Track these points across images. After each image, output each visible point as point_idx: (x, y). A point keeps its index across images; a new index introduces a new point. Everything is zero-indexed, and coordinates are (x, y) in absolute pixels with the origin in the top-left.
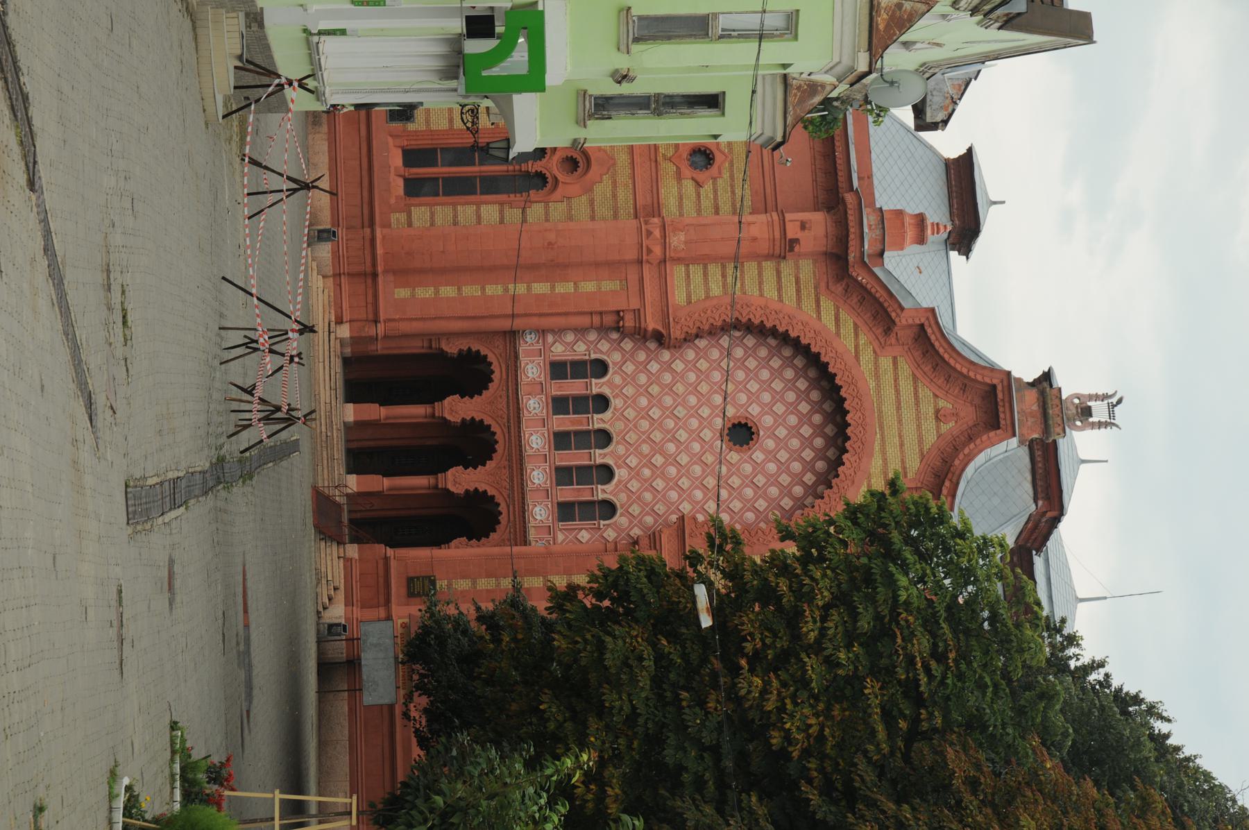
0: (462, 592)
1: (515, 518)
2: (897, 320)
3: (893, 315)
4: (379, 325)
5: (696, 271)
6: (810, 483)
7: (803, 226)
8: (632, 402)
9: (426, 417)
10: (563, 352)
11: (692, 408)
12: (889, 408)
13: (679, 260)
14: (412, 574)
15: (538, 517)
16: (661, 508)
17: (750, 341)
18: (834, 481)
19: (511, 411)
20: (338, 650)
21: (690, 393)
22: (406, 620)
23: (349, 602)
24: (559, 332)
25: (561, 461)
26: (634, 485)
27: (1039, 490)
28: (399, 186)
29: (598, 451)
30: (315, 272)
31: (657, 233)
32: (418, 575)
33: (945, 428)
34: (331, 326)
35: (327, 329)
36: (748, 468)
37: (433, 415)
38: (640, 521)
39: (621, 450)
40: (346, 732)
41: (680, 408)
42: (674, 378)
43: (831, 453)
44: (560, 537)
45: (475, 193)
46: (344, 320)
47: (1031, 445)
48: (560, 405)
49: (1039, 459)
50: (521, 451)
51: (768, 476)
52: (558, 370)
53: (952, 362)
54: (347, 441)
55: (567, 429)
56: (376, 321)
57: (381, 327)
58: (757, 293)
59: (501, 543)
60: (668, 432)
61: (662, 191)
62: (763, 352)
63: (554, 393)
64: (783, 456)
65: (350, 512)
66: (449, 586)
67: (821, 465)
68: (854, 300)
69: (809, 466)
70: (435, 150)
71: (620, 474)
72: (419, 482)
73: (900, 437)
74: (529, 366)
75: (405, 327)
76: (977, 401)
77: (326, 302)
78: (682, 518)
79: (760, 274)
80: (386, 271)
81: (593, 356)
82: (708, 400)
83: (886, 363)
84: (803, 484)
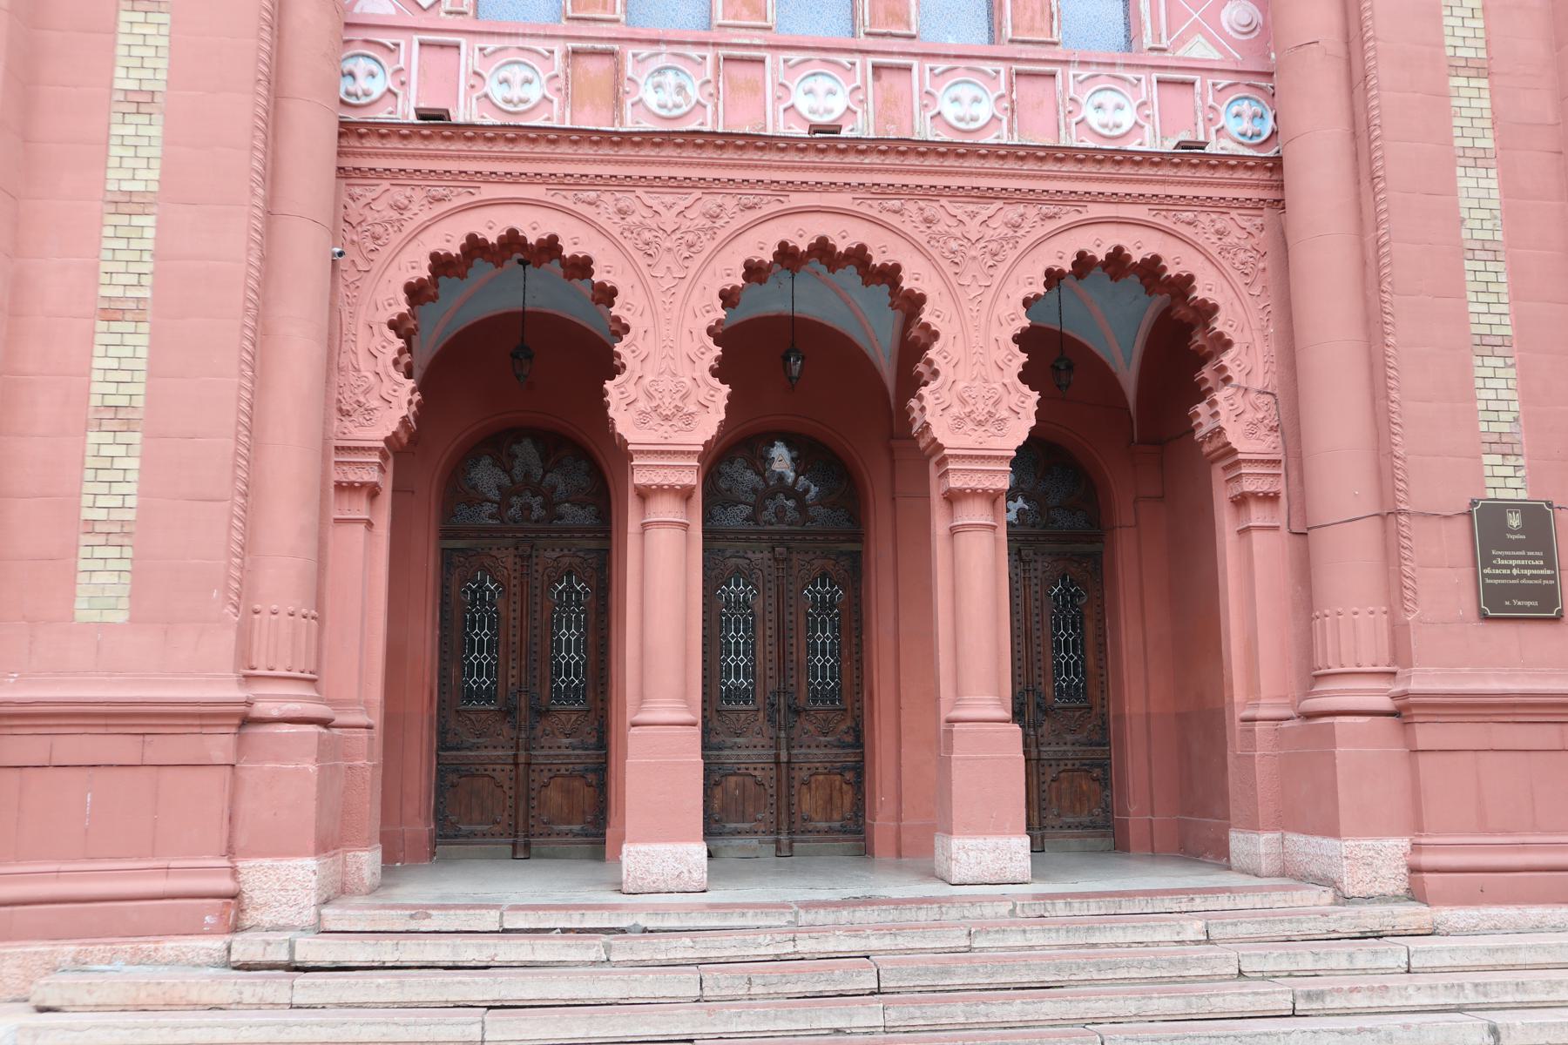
0: (1527, 397)
1: (1140, 199)
4: (262, 709)
15: (1127, 118)
19: (695, 173)
35: (277, 987)
44: (1199, 50)
46: (225, 884)
63: (619, 13)
66: (1503, 446)
74: (498, 93)
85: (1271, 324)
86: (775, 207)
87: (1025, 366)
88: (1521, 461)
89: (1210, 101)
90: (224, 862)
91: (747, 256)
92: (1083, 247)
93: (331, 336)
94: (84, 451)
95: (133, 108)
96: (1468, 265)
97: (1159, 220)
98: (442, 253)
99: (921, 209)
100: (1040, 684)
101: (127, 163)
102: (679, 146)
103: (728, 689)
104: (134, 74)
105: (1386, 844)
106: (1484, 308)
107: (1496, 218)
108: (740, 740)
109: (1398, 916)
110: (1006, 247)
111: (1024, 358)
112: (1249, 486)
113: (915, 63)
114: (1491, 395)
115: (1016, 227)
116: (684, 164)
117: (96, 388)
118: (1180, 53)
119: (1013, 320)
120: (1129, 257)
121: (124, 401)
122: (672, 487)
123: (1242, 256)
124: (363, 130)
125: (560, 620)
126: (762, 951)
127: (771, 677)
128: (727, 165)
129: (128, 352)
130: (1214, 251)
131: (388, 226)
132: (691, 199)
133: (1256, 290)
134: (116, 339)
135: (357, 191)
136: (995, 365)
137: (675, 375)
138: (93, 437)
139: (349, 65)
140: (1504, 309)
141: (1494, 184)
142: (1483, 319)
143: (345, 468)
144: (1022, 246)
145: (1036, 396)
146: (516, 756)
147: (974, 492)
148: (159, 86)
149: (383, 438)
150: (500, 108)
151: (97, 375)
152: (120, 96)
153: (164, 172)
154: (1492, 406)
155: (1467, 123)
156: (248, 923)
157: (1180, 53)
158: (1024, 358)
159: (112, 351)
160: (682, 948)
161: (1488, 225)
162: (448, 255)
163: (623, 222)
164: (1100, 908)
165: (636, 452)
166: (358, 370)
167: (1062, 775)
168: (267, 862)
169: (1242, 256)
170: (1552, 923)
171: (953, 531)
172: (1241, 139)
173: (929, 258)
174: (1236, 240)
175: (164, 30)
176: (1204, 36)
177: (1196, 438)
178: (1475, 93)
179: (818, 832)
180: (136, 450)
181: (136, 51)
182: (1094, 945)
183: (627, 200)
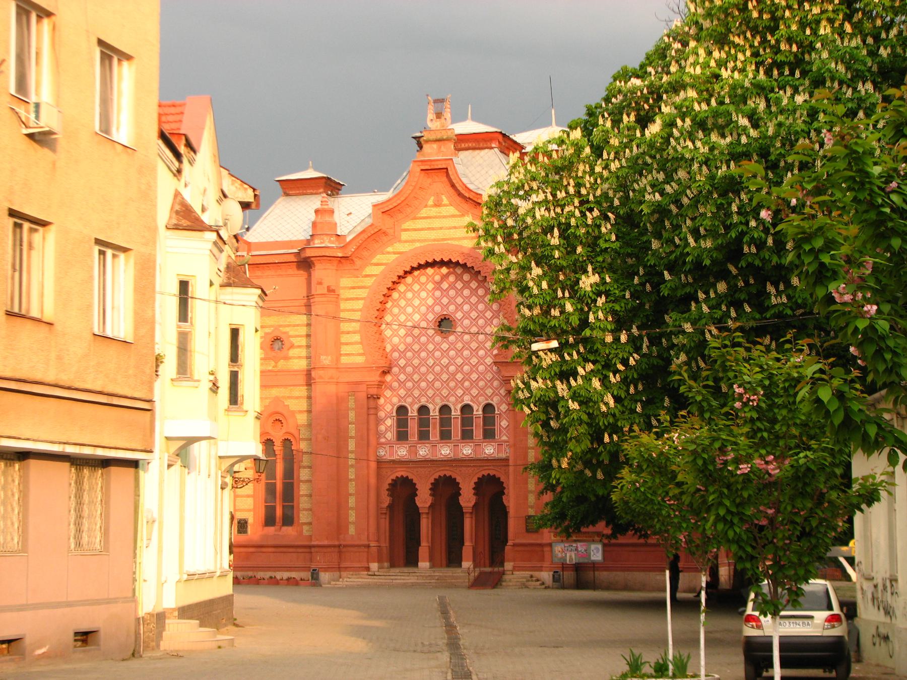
2: (379, 228)
3: (376, 230)
5: (345, 349)
6: (477, 284)
7: (320, 283)
8: (423, 392)
9: (428, 518)
11: (428, 355)
12: (432, 235)
13: (338, 360)
14: (524, 530)
15: (492, 451)
16: (489, 376)
17: (388, 318)
18: (476, 269)
20: (569, 576)
21: (419, 355)
22: (552, 534)
23: (540, 569)
24: (379, 435)
25: (458, 436)
26: (474, 392)
27: (485, 146)
28: (288, 530)
29: (453, 413)
30: (338, 583)
31: (321, 372)
32: (524, 526)
33: (445, 201)
36: (466, 322)
37: (428, 513)
38: (497, 389)
39: (452, 399)
40: (618, 573)
41: (428, 363)
42: (409, 365)
43: (459, 271)
44: (504, 438)
45: (292, 483)
47: (458, 150)
48: (424, 436)
49: (467, 145)
50: (451, 461)
51: (471, 310)
52: (402, 436)
53: (405, 196)
54: (441, 566)
56: (368, 546)
57: (372, 544)
58: (359, 313)
59: (507, 474)
60: (442, 370)
61: (296, 368)
62: (396, 310)
64: (459, 300)
65: (485, 566)
67: (466, 277)
68: (365, 253)
69: (466, 285)
70: (266, 506)
71: (467, 400)
72: (468, 524)
73: (450, 228)
74: (399, 453)
75: (372, 529)
76: (429, 181)
78: (495, 363)
79: (349, 310)
80: (338, 539)
81: (394, 414)
82: (424, 344)
83: (404, 236)
84: (477, 288)
145: (474, 498)
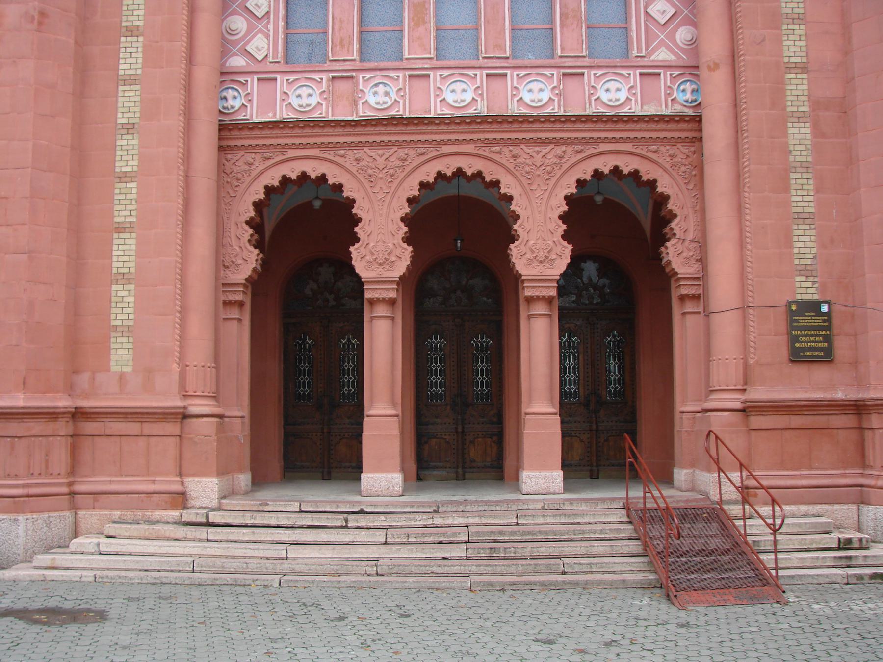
0: (822, 245)
4: (194, 410)
9: (393, 318)
10: (267, 37)
14: (784, 353)
15: (623, 96)
19: (393, 138)
30: (61, 559)
32: (783, 340)
34: (193, 519)
35: (202, 532)
44: (663, 55)
46: (177, 488)
55: (433, 34)
57: (197, 407)
63: (355, 56)
66: (806, 272)
74: (295, 102)
77: (134, 529)
80: (70, 389)
85: (698, 204)
86: (435, 153)
87: (565, 231)
88: (816, 280)
89: (669, 84)
90: (178, 479)
91: (421, 180)
92: (597, 167)
93: (218, 230)
94: (111, 294)
95: (125, 132)
96: (792, 175)
97: (638, 151)
98: (270, 185)
99: (511, 151)
100: (599, 390)
101: (124, 158)
102: (385, 125)
103: (431, 393)
104: (126, 115)
105: (733, 475)
106: (800, 198)
107: (809, 149)
108: (438, 420)
109: (733, 510)
110: (555, 169)
111: (564, 227)
112: (684, 291)
113: (508, 72)
114: (802, 244)
115: (561, 158)
116: (388, 134)
117: (115, 265)
118: (652, 58)
119: (559, 207)
120: (622, 171)
121: (126, 270)
122: (384, 300)
123: (683, 168)
124: (231, 127)
125: (344, 357)
126: (417, 523)
127: (454, 387)
128: (410, 133)
129: (127, 247)
130: (668, 166)
131: (244, 173)
132: (392, 151)
133: (691, 187)
134: (122, 242)
135: (229, 157)
136: (549, 231)
137: (384, 242)
138: (114, 287)
139: (224, 94)
140: (811, 198)
141: (808, 131)
142: (800, 204)
143: (227, 294)
144: (564, 168)
145: (570, 247)
146: (323, 429)
147: (538, 297)
148: (137, 120)
149: (244, 278)
150: (297, 110)
151: (115, 259)
152: (119, 127)
153: (140, 160)
154: (802, 250)
155: (795, 98)
156: (190, 505)
157: (651, 59)
158: (564, 227)
159: (121, 247)
160: (380, 521)
161: (804, 153)
162: (273, 186)
163: (358, 165)
164: (587, 506)
165: (366, 282)
166: (232, 246)
167: (610, 438)
168: (196, 479)
169: (683, 168)
170: (812, 513)
171: (529, 317)
172: (685, 104)
173: (515, 177)
174: (680, 160)
175: (138, 93)
176: (666, 48)
177: (663, 263)
178: (800, 82)
179: (479, 468)
180: (132, 293)
181: (126, 105)
182: (579, 523)
183: (359, 154)
